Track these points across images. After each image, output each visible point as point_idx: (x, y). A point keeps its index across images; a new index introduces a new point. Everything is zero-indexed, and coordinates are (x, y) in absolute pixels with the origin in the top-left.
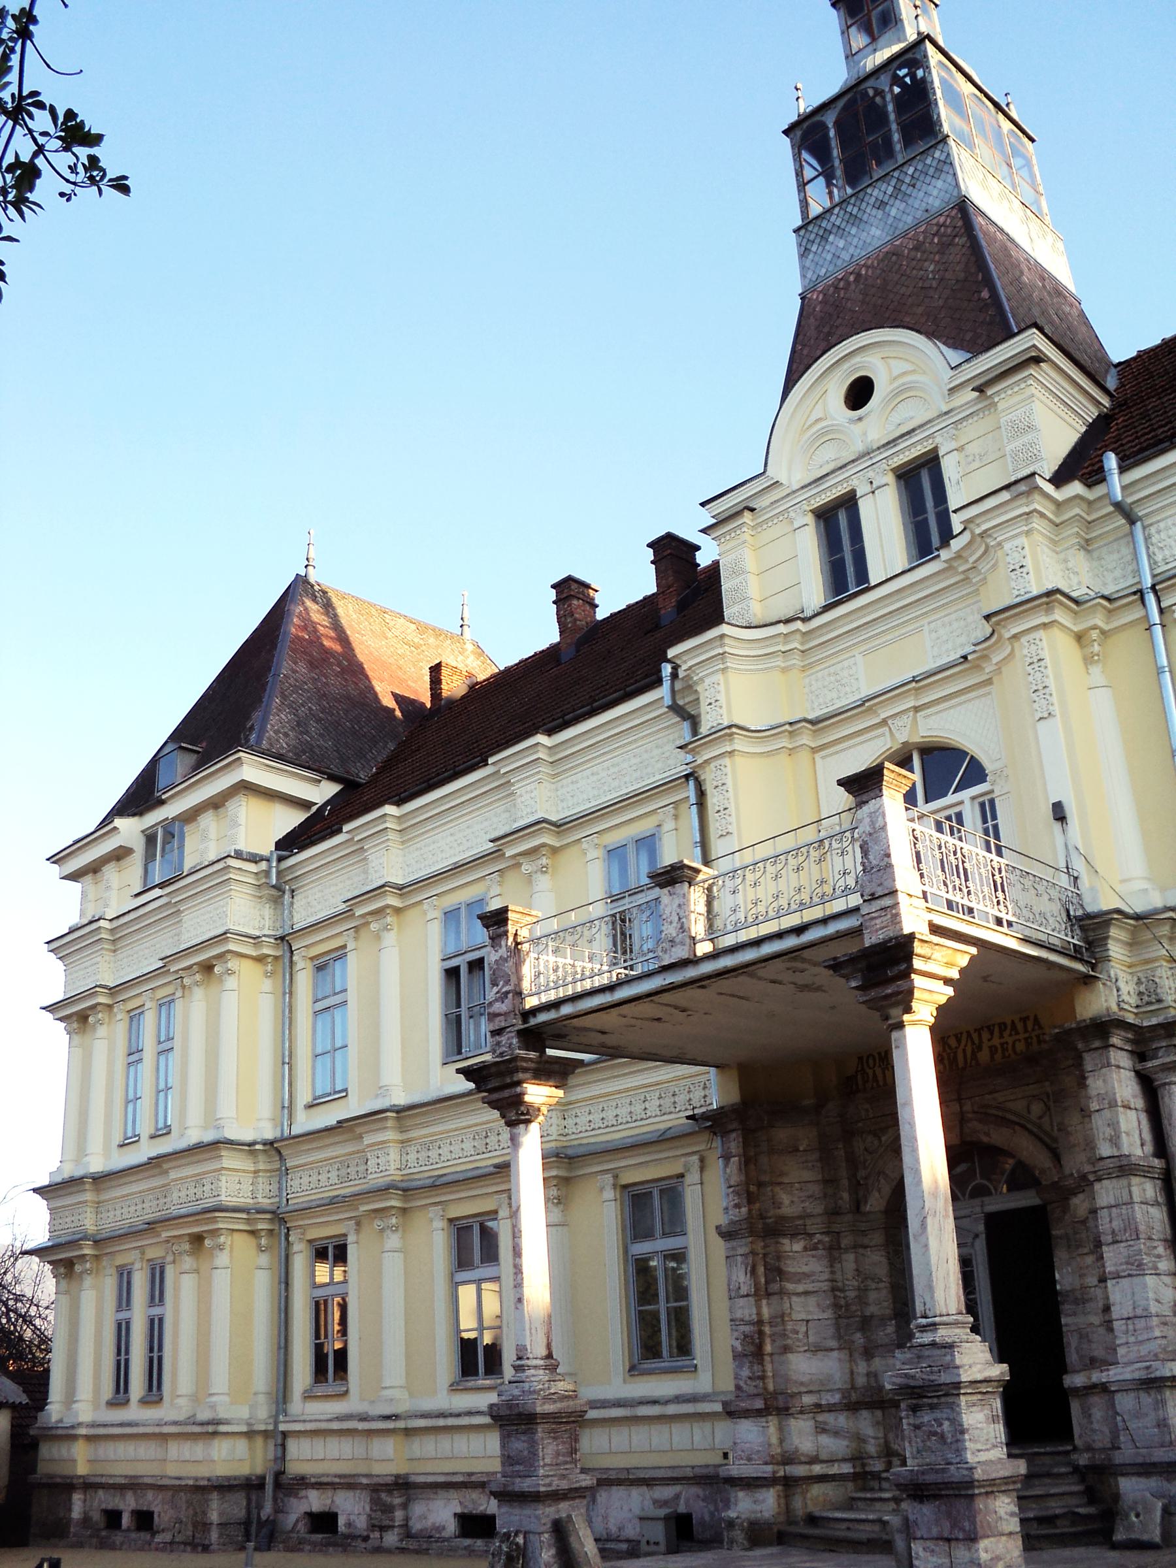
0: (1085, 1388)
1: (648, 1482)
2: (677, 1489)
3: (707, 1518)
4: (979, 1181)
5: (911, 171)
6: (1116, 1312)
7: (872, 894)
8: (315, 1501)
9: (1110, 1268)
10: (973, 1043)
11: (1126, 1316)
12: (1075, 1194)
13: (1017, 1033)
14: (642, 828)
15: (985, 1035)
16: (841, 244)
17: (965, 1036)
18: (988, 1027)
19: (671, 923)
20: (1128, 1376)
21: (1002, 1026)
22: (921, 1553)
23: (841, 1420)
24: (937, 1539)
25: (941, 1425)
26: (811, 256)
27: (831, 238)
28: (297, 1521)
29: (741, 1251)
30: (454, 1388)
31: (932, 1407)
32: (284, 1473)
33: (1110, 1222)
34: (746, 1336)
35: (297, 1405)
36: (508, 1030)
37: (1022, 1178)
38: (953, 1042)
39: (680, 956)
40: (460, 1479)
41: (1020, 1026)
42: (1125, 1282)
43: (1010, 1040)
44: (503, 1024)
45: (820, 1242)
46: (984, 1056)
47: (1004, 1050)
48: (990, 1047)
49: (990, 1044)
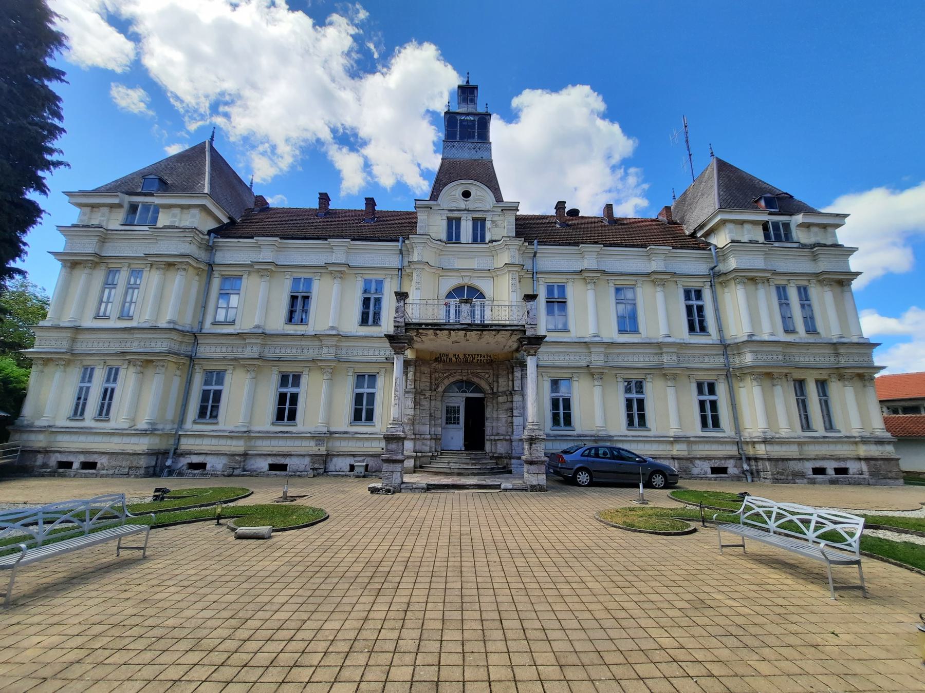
1: (354, 456)
2: (364, 458)
3: (374, 465)
6: (514, 424)
8: (195, 459)
9: (514, 414)
14: (380, 277)
15: (476, 356)
21: (481, 355)
23: (428, 442)
28: (183, 466)
30: (273, 424)
31: (535, 444)
32: (177, 449)
35: (189, 425)
37: (478, 389)
38: (467, 356)
46: (475, 361)
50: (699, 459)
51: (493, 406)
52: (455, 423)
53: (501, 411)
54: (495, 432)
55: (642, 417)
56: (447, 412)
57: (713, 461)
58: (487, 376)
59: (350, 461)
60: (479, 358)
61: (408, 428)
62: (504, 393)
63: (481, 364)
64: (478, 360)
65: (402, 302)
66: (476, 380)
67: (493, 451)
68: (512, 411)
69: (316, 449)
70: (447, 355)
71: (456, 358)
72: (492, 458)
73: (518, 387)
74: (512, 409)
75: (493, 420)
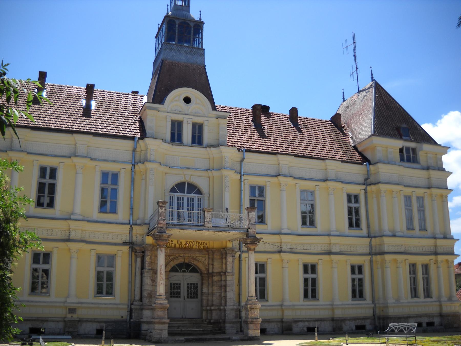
4: (184, 269)
5: (195, 50)
6: (228, 297)
9: (227, 290)
10: (192, 244)
12: (215, 276)
15: (195, 243)
16: (175, 54)
17: (191, 242)
21: (199, 243)
26: (166, 52)
27: (172, 51)
34: (148, 293)
40: (34, 319)
42: (230, 293)
43: (200, 246)
44: (163, 226)
47: (198, 247)
50: (349, 320)
51: (208, 283)
52: (177, 297)
53: (215, 288)
54: (210, 303)
56: (171, 287)
57: (357, 321)
58: (203, 259)
59: (96, 326)
60: (197, 245)
61: (148, 300)
62: (219, 274)
63: (200, 250)
64: (196, 246)
65: (164, 208)
66: (195, 262)
67: (209, 318)
68: (225, 288)
69: (69, 316)
70: (172, 242)
71: (180, 245)
72: (210, 323)
73: (230, 269)
74: (225, 286)
75: (208, 294)
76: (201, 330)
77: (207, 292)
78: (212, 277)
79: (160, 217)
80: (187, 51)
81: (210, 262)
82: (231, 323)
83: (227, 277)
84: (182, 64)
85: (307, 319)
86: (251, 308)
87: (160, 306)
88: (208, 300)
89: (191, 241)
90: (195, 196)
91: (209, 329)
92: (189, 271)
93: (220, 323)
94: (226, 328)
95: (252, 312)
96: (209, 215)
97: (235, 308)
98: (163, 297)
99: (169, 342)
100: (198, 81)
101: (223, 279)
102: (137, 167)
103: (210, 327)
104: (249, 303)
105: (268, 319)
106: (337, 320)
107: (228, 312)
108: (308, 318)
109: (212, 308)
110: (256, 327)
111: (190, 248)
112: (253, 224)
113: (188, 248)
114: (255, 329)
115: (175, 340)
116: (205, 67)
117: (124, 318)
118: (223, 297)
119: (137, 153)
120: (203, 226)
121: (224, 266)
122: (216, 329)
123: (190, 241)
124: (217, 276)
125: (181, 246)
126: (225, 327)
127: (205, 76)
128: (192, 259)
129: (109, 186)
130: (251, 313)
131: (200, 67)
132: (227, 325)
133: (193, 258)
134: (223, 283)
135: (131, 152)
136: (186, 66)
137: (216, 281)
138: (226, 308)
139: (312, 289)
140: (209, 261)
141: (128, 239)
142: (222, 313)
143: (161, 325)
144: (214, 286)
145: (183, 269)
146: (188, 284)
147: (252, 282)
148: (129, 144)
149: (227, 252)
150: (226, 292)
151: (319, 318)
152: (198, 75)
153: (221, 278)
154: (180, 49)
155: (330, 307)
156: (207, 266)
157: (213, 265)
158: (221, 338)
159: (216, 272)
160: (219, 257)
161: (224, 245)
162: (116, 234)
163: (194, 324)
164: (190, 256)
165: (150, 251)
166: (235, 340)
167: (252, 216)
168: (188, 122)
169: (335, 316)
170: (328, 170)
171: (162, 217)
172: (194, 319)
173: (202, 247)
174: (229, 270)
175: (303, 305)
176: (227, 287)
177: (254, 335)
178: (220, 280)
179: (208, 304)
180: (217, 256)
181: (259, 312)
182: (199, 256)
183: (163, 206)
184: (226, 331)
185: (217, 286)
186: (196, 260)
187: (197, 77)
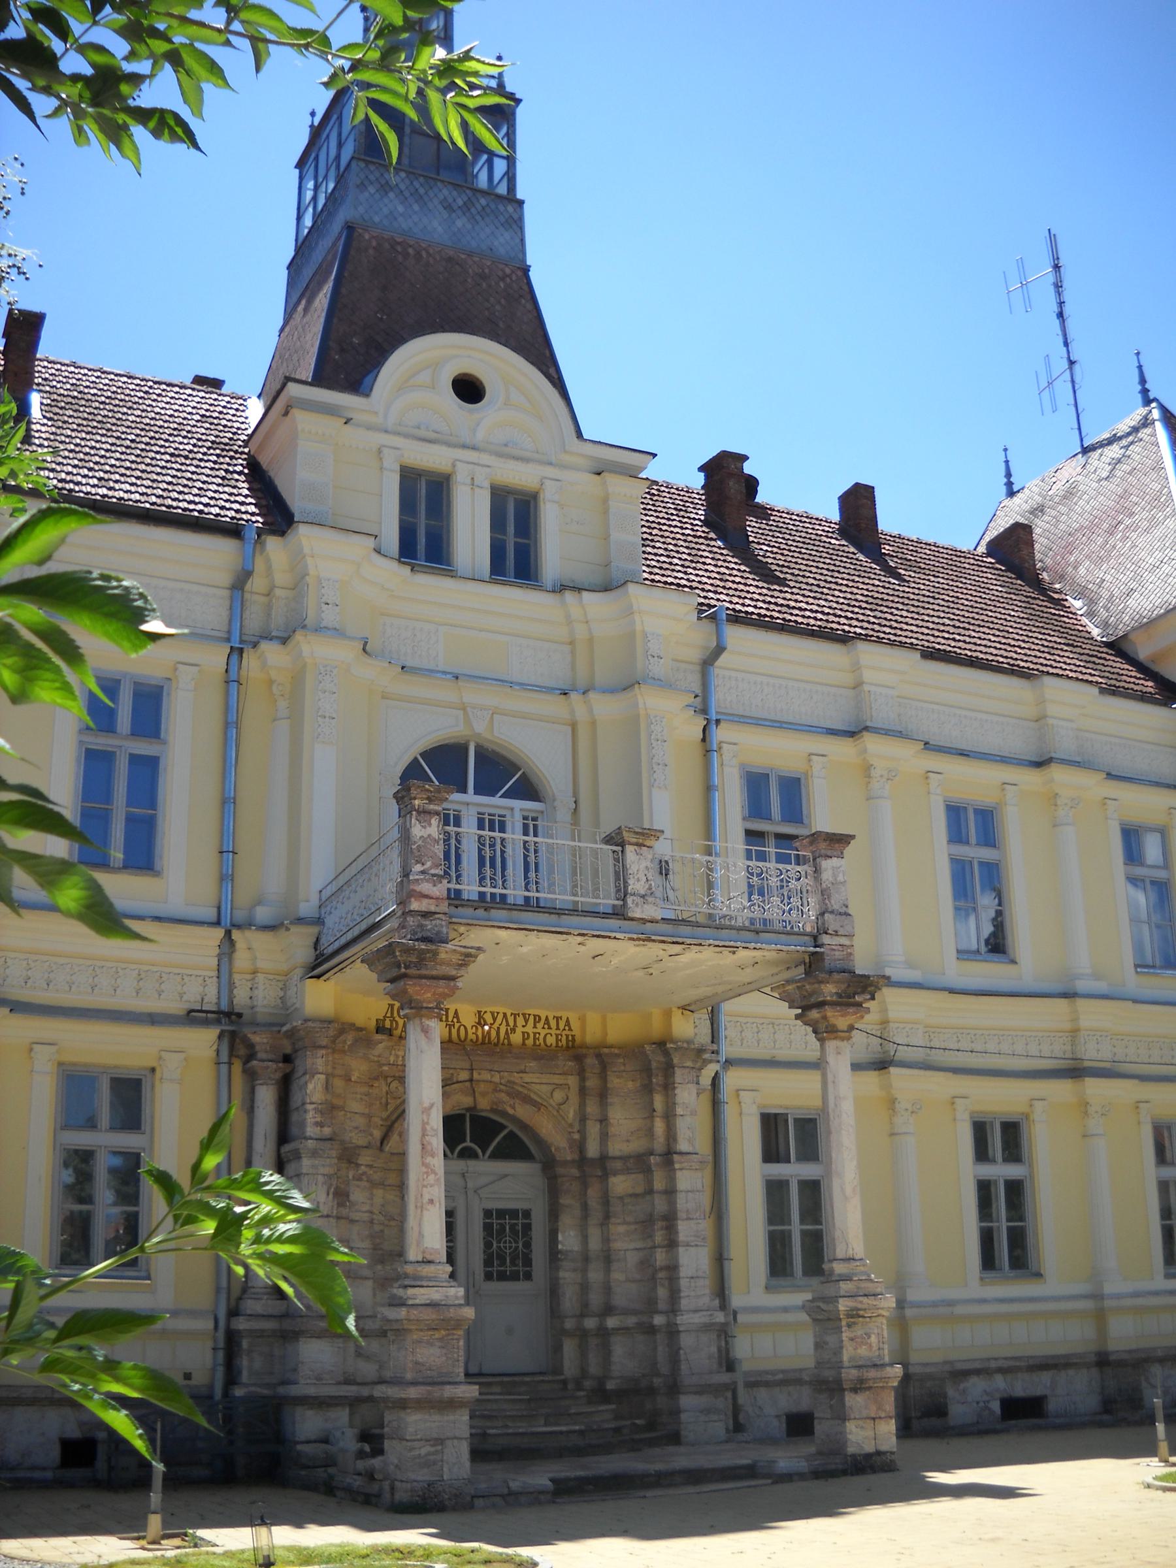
0: (613, 1329)
4: (468, 1143)
5: (483, 201)
7: (836, 932)
9: (682, 1237)
10: (508, 1025)
11: (690, 1275)
12: (615, 1175)
13: (550, 1028)
15: (520, 1021)
16: (401, 209)
17: (500, 1017)
18: (524, 1015)
19: (638, 880)
20: (696, 1321)
21: (537, 1019)
22: (854, 1430)
24: (865, 1418)
25: (869, 1337)
26: (366, 194)
27: (391, 195)
29: (326, 1170)
33: (687, 1202)
36: (437, 916)
39: (653, 915)
41: (553, 1023)
42: (692, 1250)
43: (543, 1032)
44: (433, 908)
45: (364, 1173)
46: (516, 1038)
47: (535, 1039)
48: (523, 1033)
49: (525, 1030)
50: (1162, 1361)
51: (585, 1207)
53: (621, 1229)
54: (596, 1299)
55: (1018, 1239)
58: (558, 1096)
62: (639, 1163)
63: (543, 1055)
65: (434, 821)
66: (522, 1111)
72: (601, 1394)
73: (690, 1141)
76: (575, 1432)
77: (576, 1248)
78: (605, 1175)
79: (418, 862)
80: (450, 200)
81: (589, 1110)
82: (701, 1390)
83: (679, 1174)
84: (431, 251)
85: (1000, 1363)
86: (854, 1315)
87: (429, 1315)
88: (584, 1287)
89: (502, 1010)
90: (512, 809)
91: (606, 1426)
92: (488, 1153)
93: (651, 1391)
94: (684, 1417)
95: (859, 1331)
96: (644, 864)
97: (718, 1320)
98: (440, 1267)
99: (479, 1502)
100: (501, 325)
101: (659, 1184)
102: (251, 660)
103: (604, 1415)
104: (842, 1293)
105: (795, 1371)
106: (1121, 1364)
107: (686, 1341)
108: (1006, 1359)
109: (611, 1322)
110: (880, 1408)
111: (496, 1045)
112: (840, 914)
113: (490, 1042)
114: (873, 1415)
115: (506, 1491)
116: (526, 270)
117: (199, 1379)
118: (661, 1269)
119: (255, 597)
120: (619, 913)
121: (659, 1126)
122: (638, 1422)
123: (495, 1009)
124: (627, 1171)
125: (454, 1032)
126: (676, 1412)
127: (529, 306)
128: (509, 1094)
129: (117, 742)
130: (852, 1339)
131: (508, 271)
132: (686, 1401)
133: (514, 1094)
134: (660, 1205)
135: (226, 593)
136: (450, 259)
137: (621, 1198)
138: (679, 1320)
139: (1009, 1229)
140: (582, 1105)
141: (207, 994)
142: (660, 1348)
143: (436, 1417)
144: (613, 1220)
145: (464, 1141)
146: (488, 1213)
147: (849, 1190)
148: (221, 549)
149: (676, 1061)
150: (672, 1244)
151: (1046, 1357)
152: (503, 301)
153: (650, 1182)
154: (422, 191)
155: (1089, 1305)
156: (577, 1127)
157: (604, 1120)
158: (713, 1470)
159: (618, 1154)
160: (630, 1085)
161: (656, 1029)
162: (155, 969)
163: (529, 1400)
164: (496, 1079)
165: (323, 1052)
166: (787, 1478)
167: (835, 876)
168: (476, 482)
169: (1112, 1346)
170: (1050, 721)
171: (429, 864)
172: (527, 1379)
173: (551, 1040)
174: (683, 1146)
175: (983, 1301)
176: (679, 1222)
177: (869, 1448)
178: (640, 1190)
179: (585, 1305)
180: (622, 1083)
181: (886, 1335)
182: (537, 1081)
183: (432, 807)
184: (682, 1433)
185: (630, 1219)
186: (527, 1100)
187: (498, 307)
